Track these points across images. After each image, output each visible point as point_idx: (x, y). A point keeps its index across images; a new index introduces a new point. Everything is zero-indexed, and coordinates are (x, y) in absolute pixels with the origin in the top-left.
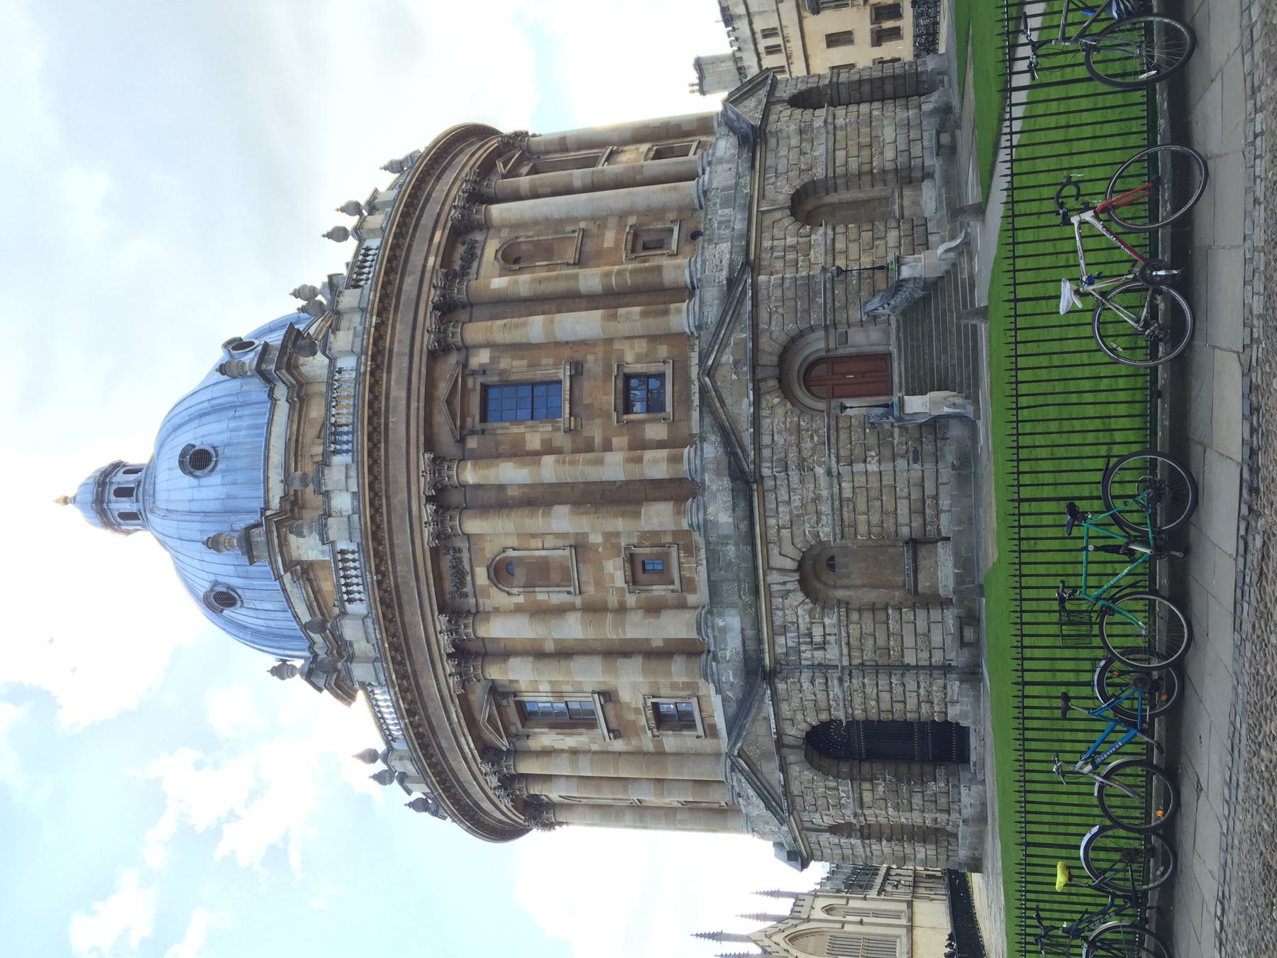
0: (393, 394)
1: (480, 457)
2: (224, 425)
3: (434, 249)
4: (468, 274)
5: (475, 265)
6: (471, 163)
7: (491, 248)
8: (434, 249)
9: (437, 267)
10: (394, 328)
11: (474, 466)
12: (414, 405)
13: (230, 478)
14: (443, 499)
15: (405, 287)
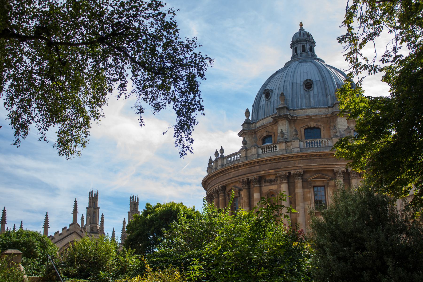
0: (232, 174)
1: (225, 200)
2: (276, 98)
3: (266, 172)
4: (265, 183)
5: (268, 184)
6: (313, 167)
7: (274, 187)
8: (266, 172)
9: (261, 175)
10: (244, 168)
11: (221, 200)
12: (229, 180)
13: (264, 107)
14: (217, 192)
15: (255, 167)
